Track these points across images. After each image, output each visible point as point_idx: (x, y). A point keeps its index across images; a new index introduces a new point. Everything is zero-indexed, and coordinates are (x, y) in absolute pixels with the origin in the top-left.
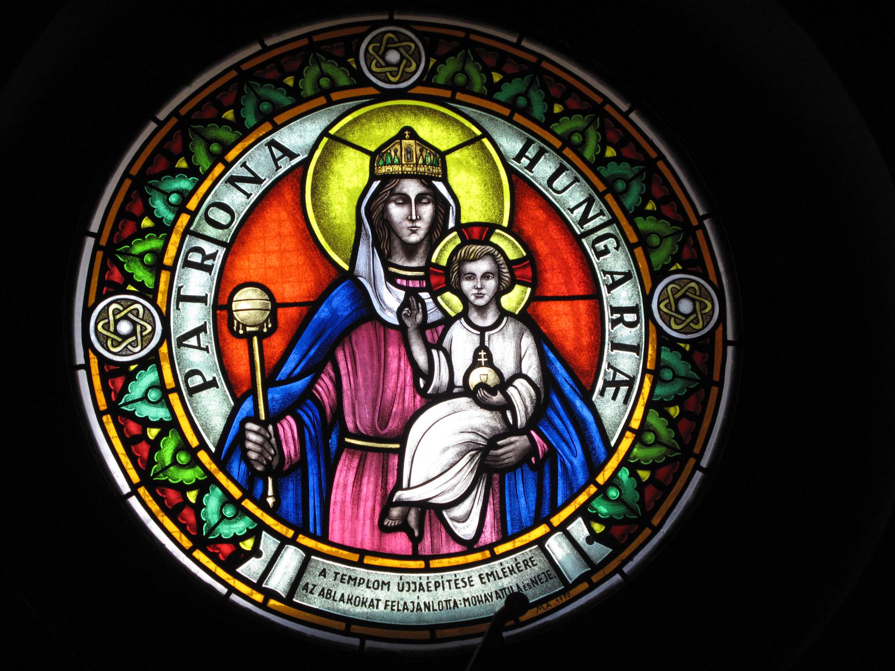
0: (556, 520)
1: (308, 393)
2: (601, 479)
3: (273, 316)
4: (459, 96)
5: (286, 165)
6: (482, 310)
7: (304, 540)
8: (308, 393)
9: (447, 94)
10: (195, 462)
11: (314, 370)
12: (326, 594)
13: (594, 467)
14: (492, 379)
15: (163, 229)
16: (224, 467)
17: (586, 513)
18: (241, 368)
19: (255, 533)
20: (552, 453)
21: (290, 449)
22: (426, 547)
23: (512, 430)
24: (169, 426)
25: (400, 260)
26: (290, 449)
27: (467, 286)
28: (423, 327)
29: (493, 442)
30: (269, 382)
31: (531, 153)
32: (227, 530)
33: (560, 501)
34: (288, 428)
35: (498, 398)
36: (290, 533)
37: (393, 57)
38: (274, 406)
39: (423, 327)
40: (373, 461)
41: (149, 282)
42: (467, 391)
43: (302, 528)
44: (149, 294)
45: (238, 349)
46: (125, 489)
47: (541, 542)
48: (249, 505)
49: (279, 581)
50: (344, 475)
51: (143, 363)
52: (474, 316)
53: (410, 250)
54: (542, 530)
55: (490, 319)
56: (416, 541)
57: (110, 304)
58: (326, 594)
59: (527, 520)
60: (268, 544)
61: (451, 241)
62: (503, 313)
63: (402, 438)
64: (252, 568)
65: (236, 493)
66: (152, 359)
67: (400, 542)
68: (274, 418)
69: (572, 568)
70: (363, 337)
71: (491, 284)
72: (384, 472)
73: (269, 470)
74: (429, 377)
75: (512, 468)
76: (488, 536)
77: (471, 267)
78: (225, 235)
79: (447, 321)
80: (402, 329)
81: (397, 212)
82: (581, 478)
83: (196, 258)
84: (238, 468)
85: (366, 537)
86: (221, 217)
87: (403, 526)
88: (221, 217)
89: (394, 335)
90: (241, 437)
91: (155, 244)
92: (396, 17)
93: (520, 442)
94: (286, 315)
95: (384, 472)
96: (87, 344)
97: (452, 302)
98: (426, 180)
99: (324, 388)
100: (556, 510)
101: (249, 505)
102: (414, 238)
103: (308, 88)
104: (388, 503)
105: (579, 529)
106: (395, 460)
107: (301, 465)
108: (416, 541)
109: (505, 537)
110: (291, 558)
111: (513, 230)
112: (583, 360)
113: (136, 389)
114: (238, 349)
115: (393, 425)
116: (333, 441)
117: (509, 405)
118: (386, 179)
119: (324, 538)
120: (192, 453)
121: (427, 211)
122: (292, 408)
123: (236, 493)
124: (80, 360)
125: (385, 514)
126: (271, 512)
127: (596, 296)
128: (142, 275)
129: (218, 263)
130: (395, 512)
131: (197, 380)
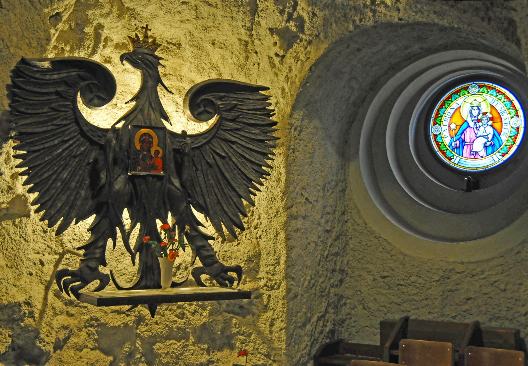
0: (494, 153)
1: (461, 137)
2: (501, 147)
3: (456, 127)
4: (483, 94)
5: (458, 106)
6: (485, 125)
7: (460, 156)
8: (461, 137)
9: (481, 94)
10: (446, 147)
11: (462, 134)
12: (462, 164)
13: (500, 146)
14: (486, 134)
15: (442, 116)
16: (449, 147)
17: (498, 152)
18: (452, 135)
19: (453, 156)
20: (494, 144)
21: (458, 145)
22: (476, 157)
23: (489, 141)
24: (443, 142)
25: (473, 118)
26: (458, 145)
27: (483, 121)
28: (476, 128)
29: (486, 143)
30: (456, 136)
31: (493, 101)
32: (449, 156)
33: (495, 150)
34: (458, 142)
35: (487, 137)
36: (458, 156)
37: (473, 89)
38: (456, 139)
39: (476, 128)
40: (469, 146)
41: (440, 124)
42: (482, 136)
43: (460, 155)
44: (440, 125)
45: (451, 132)
46: (437, 151)
47: (492, 156)
48: (452, 152)
49: (456, 162)
50: (465, 148)
51: (439, 134)
52: (484, 126)
53: (475, 117)
54: (492, 154)
55: (486, 125)
56: (475, 156)
57: (435, 127)
58: (462, 164)
59: (490, 153)
60: (455, 157)
61: (481, 115)
62: (488, 125)
63: (473, 143)
64: (453, 160)
65: (451, 151)
66: (440, 134)
67: (473, 157)
68: (456, 141)
69: (496, 160)
70: (468, 129)
71: (486, 121)
72: (471, 147)
73: (455, 148)
74: (477, 134)
75: (488, 146)
76: (485, 155)
77: (483, 119)
78: (450, 116)
79: (480, 127)
80: (474, 128)
81: (473, 112)
82: (498, 147)
83: (446, 120)
84: (451, 147)
85: (468, 156)
86: (449, 114)
87: (473, 155)
88: (449, 114)
89: (472, 129)
90: (452, 144)
91: (441, 118)
92: (474, 83)
93: (490, 143)
94: (458, 127)
95: (471, 147)
96: (432, 132)
97: (480, 124)
98: (478, 107)
99: (463, 136)
100: (494, 152)
101: (452, 152)
102: (475, 115)
103: (461, 95)
104: (471, 152)
105: (498, 154)
106: (472, 146)
107: (459, 147)
108: (475, 156)
109: (487, 156)
110: (458, 159)
111: (491, 113)
112: (499, 131)
113: (438, 138)
114: (451, 132)
115: (472, 141)
116: (464, 144)
117: (488, 138)
118: (472, 107)
119: (462, 156)
120: (445, 146)
121: (478, 111)
122: (458, 139)
123: (451, 151)
124: (431, 134)
125: (470, 153)
126: (456, 153)
127: (502, 122)
128: (439, 123)
129: (448, 121)
130: (472, 153)
131: (445, 136)
